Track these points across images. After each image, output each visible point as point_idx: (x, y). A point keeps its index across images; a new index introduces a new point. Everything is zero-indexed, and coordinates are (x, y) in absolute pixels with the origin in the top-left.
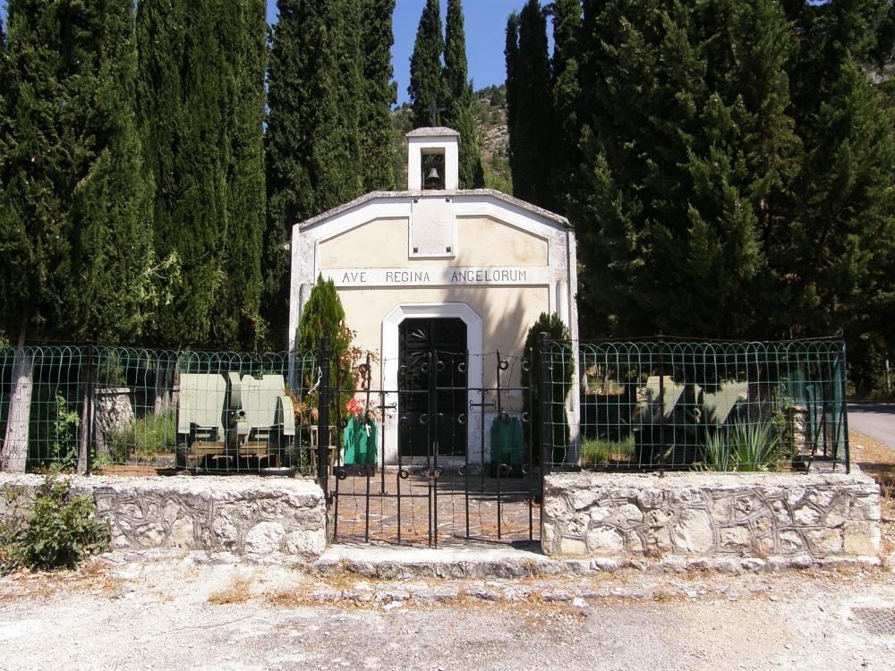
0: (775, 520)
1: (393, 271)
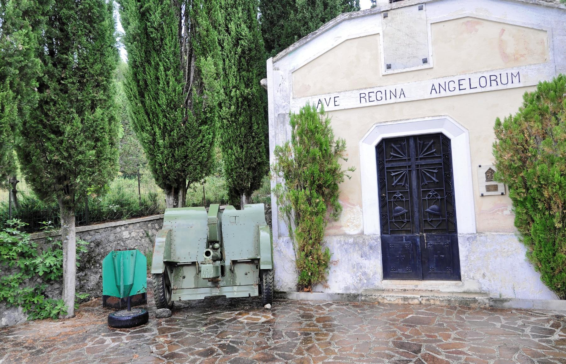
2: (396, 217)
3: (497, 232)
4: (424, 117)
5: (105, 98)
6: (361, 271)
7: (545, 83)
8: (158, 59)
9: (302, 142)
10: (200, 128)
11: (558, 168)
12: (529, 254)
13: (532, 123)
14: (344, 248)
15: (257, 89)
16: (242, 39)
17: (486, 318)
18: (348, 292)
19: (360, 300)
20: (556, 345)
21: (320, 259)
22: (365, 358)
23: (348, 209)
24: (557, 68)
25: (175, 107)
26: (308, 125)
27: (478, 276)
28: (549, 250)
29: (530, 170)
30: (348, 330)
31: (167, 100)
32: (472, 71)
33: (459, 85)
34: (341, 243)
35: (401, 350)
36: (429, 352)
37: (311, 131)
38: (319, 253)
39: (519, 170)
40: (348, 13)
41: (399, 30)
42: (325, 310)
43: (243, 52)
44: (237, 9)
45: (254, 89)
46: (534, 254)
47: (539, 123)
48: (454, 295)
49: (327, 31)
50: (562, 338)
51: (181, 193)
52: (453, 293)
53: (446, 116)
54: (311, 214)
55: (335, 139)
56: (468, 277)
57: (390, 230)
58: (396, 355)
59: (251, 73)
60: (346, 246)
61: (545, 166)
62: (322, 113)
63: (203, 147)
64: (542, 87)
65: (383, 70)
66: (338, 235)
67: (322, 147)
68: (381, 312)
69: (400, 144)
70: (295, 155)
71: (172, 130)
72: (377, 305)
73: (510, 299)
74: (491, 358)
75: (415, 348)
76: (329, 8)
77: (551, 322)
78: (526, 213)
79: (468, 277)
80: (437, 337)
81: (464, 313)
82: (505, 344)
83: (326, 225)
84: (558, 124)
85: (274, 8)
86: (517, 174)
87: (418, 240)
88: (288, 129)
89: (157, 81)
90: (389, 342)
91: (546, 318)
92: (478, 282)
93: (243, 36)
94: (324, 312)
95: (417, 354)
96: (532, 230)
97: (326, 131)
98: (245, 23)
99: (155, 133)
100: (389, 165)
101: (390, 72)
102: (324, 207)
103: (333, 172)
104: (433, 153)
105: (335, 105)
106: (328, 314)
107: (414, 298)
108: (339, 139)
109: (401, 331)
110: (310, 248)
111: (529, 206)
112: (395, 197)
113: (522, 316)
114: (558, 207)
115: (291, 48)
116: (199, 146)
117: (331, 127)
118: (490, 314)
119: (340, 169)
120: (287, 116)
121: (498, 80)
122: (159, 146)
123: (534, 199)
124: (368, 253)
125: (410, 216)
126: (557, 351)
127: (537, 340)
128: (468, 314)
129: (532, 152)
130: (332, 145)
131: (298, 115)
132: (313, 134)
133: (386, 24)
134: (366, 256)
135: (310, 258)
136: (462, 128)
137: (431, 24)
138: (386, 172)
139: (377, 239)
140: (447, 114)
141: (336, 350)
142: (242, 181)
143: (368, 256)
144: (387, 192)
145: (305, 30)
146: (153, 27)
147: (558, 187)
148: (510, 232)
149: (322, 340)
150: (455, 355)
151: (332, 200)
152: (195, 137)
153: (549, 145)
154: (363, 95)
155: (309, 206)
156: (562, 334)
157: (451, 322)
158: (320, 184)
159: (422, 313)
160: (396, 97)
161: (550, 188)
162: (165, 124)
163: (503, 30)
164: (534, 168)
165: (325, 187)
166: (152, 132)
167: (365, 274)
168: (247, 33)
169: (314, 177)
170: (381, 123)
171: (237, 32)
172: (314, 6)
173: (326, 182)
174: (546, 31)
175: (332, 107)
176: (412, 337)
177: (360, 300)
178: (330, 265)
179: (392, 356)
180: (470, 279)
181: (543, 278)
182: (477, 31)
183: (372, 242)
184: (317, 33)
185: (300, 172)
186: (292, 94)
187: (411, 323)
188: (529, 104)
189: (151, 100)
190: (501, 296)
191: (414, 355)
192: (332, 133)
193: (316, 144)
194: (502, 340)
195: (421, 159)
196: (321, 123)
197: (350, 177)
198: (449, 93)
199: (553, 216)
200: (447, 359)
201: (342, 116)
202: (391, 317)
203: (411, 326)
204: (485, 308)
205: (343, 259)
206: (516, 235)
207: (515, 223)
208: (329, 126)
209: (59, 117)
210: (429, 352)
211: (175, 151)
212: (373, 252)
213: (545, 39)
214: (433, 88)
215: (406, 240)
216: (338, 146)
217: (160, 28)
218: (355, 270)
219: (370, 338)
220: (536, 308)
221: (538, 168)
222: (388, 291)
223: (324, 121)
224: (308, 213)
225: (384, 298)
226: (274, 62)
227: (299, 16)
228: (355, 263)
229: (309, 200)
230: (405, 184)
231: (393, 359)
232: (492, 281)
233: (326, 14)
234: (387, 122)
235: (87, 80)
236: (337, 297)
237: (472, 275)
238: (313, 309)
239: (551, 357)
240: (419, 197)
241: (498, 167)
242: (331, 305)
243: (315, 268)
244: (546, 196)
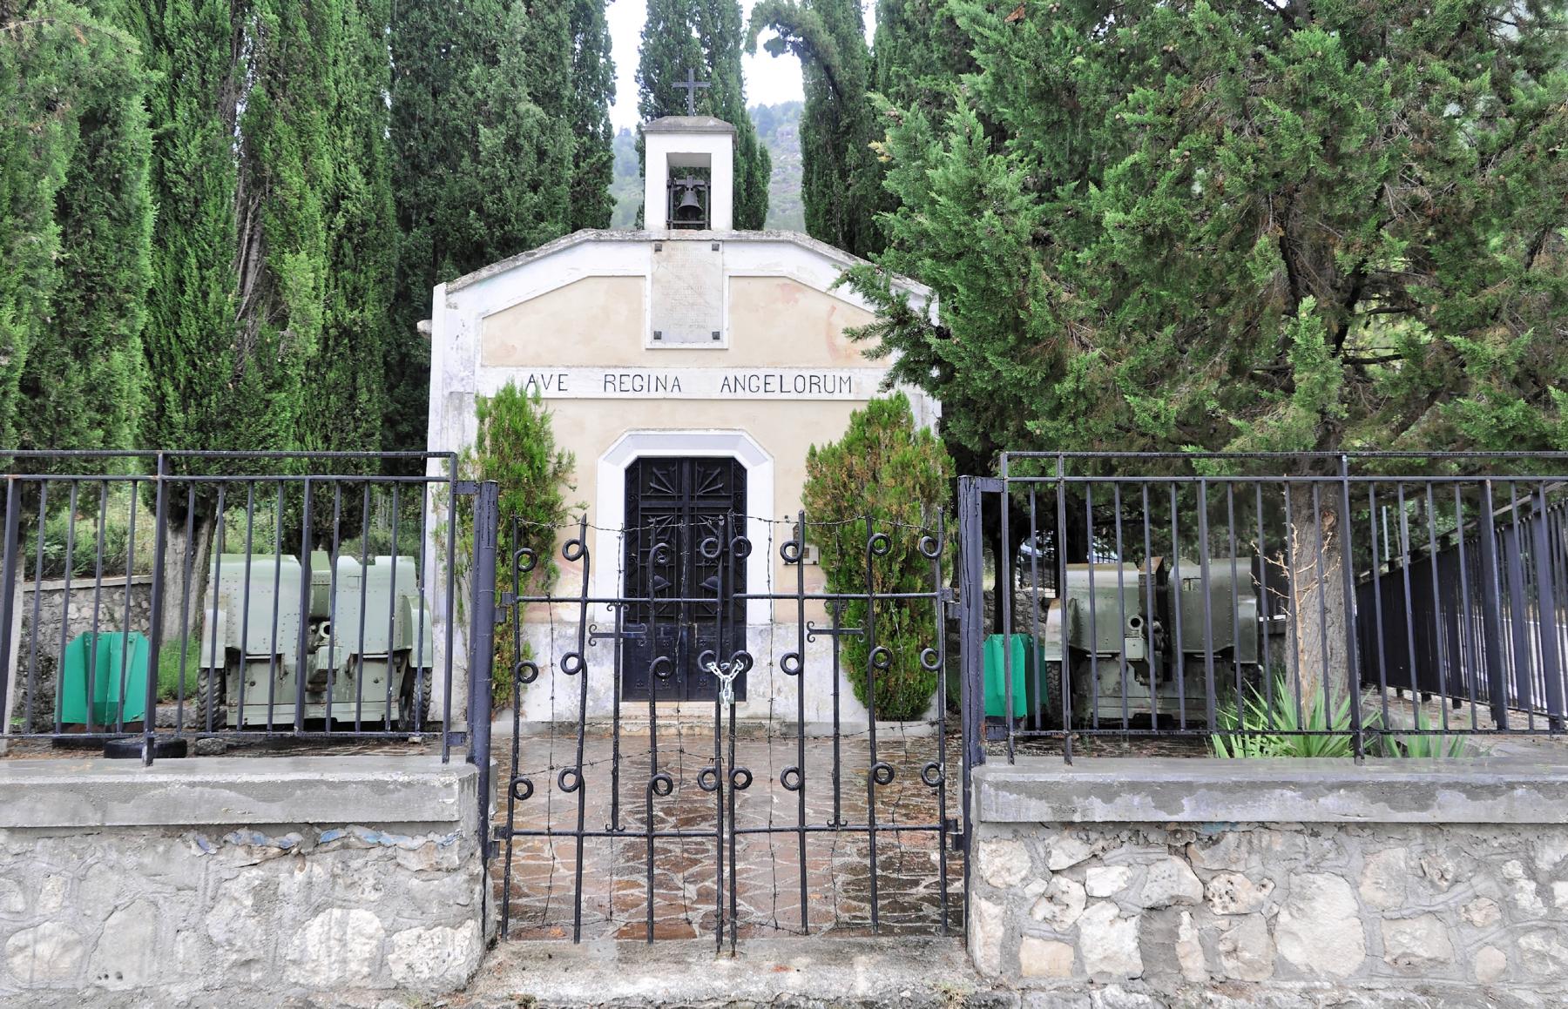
0: (1508, 905)
1: (618, 373)
5: (127, 332)
8: (185, 241)
10: (268, 396)
15: (375, 315)
16: (348, 198)
25: (216, 346)
26: (510, 420)
29: (848, 528)
31: (201, 330)
37: (516, 432)
40: (594, 231)
41: (679, 278)
43: (350, 227)
44: (340, 128)
45: (368, 314)
49: (554, 253)
51: (205, 529)
55: (556, 451)
59: (362, 276)
62: (537, 400)
63: (273, 436)
65: (647, 340)
71: (207, 394)
76: (548, 161)
85: (426, 136)
88: (467, 422)
89: (177, 286)
93: (351, 192)
97: (541, 437)
98: (358, 161)
99: (164, 396)
100: (646, 504)
101: (658, 344)
103: (550, 508)
107: (670, 726)
111: (843, 581)
115: (484, 272)
116: (263, 434)
120: (470, 400)
121: (822, 384)
122: (171, 425)
136: (765, 454)
142: (320, 516)
145: (493, 203)
146: (178, 173)
152: (257, 413)
154: (611, 378)
162: (190, 381)
163: (834, 308)
166: (158, 393)
168: (361, 186)
171: (338, 179)
172: (517, 156)
175: (552, 392)
182: (796, 301)
184: (535, 254)
186: (479, 357)
189: (159, 325)
195: (699, 497)
198: (749, 395)
201: (571, 410)
208: (546, 426)
209: (40, 362)
211: (208, 438)
217: (194, 178)
223: (539, 416)
226: (448, 293)
227: (485, 171)
233: (541, 173)
235: (99, 297)
236: (540, 728)
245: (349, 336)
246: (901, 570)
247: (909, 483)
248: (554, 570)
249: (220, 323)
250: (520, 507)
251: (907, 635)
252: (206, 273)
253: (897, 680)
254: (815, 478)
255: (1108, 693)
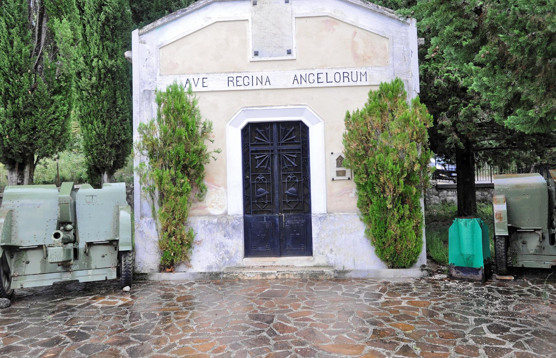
2: (258, 199)
3: (343, 212)
4: (286, 105)
6: (224, 250)
7: (386, 83)
9: (168, 121)
10: (52, 98)
11: (391, 158)
12: (367, 231)
13: (374, 117)
14: (208, 229)
15: (123, 62)
16: (106, 5)
17: (330, 288)
18: (211, 271)
19: (222, 278)
20: (382, 306)
21: (183, 239)
22: (222, 332)
23: (214, 190)
24: (395, 72)
25: (20, 71)
26: (175, 103)
27: (327, 252)
28: (382, 228)
29: (371, 159)
30: (207, 307)
31: (10, 62)
32: (329, 66)
33: (318, 78)
34: (204, 224)
35: (256, 322)
36: (280, 321)
37: (178, 110)
38: (183, 233)
39: (362, 158)
41: (267, 20)
42: (186, 289)
43: (107, 19)
45: (119, 62)
46: (371, 231)
47: (379, 118)
48: (306, 269)
49: (197, 9)
50: (387, 300)
51: (27, 169)
52: (305, 267)
53: (306, 105)
54: (176, 194)
55: (202, 120)
56: (318, 253)
57: (252, 210)
58: (251, 327)
59: (116, 44)
60: (209, 226)
61: (382, 155)
62: (190, 92)
63: (56, 119)
64: (383, 87)
65: (250, 56)
66: (202, 216)
67: (188, 127)
68: (240, 288)
69: (264, 129)
70: (161, 134)
71: (17, 97)
72: (237, 282)
73: (351, 270)
74: (331, 322)
75: (268, 319)
77: (380, 288)
78: (366, 196)
79: (318, 253)
80: (288, 307)
81: (313, 284)
82: (343, 309)
83: (190, 206)
84: (393, 120)
86: (361, 162)
87: (277, 219)
90: (245, 315)
91: (377, 285)
92: (327, 256)
94: (186, 291)
95: (270, 324)
96: (370, 209)
97: (193, 112)
100: (253, 149)
101: (257, 58)
102: (189, 188)
103: (199, 153)
104: (293, 140)
105: (203, 86)
106: (189, 293)
107: (272, 274)
108: (206, 119)
109: (257, 304)
110: (173, 228)
111: (369, 189)
112: (258, 179)
113: (359, 284)
114: (390, 191)
115: (159, 22)
116: (50, 118)
117: (198, 108)
118: (335, 284)
119: (206, 150)
120: (153, 93)
121: (350, 77)
123: (373, 183)
124: (231, 233)
125: (271, 196)
126: (382, 311)
127: (368, 304)
128: (317, 285)
129: (372, 143)
130: (199, 125)
131: (164, 93)
132: (179, 114)
133: (255, 11)
134: (229, 236)
135: (173, 238)
136: (319, 118)
137: (296, 18)
138: (250, 156)
139: (240, 219)
140: (306, 104)
141: (194, 327)
142: (104, 159)
143: (231, 236)
144: (251, 174)
145: (176, 6)
147: (390, 174)
148: (353, 213)
149: (181, 318)
150: (302, 322)
151: (197, 180)
152: (46, 107)
153: (386, 137)
154: (231, 79)
155: (173, 186)
156: (387, 297)
157: (301, 293)
158: (186, 165)
159: (278, 287)
160: (262, 83)
161: (385, 174)
163: (355, 33)
164: (374, 157)
165: (190, 167)
167: (227, 252)
169: (179, 156)
170: (247, 107)
173: (191, 162)
174: (388, 39)
175: (199, 88)
176: (267, 309)
177: (222, 278)
178: (193, 246)
179: (247, 328)
180: (320, 254)
181: (376, 251)
182: (334, 30)
183: (235, 222)
184: (187, 10)
185: (165, 152)
186: (159, 70)
187: (266, 297)
188: (372, 101)
190: (344, 268)
191: (267, 325)
192: (199, 114)
193: (182, 123)
194: (341, 306)
195: (282, 143)
196: (188, 104)
197: (216, 158)
198: (309, 85)
199: (385, 199)
200: (295, 327)
201: (210, 98)
202: (249, 292)
203: (266, 299)
204: (331, 280)
205: (207, 239)
206: (358, 215)
207: (358, 204)
208: (196, 106)
210: (280, 321)
211: (19, 121)
212: (236, 232)
213: (387, 45)
214: (296, 79)
215: (266, 220)
216: (205, 127)
218: (218, 249)
219: (228, 313)
220: (370, 276)
221: (377, 157)
222: (249, 268)
223: (191, 101)
224: (173, 194)
225: (244, 275)
226: (140, 35)
228: (218, 242)
229: (174, 180)
230: (267, 167)
231: (248, 330)
232: (338, 255)
234: (253, 107)
236: (199, 276)
237: (321, 250)
238: (174, 288)
239: (377, 316)
240: (279, 180)
241: (347, 155)
242: (193, 283)
243: (178, 249)
244: (382, 181)
245: (111, 73)
246: (405, 182)
247: (409, 131)
248: (204, 187)
249: (21, 58)
250: (182, 153)
251: (407, 220)
252: (12, 31)
253: (402, 246)
254: (350, 130)
255: (531, 252)
